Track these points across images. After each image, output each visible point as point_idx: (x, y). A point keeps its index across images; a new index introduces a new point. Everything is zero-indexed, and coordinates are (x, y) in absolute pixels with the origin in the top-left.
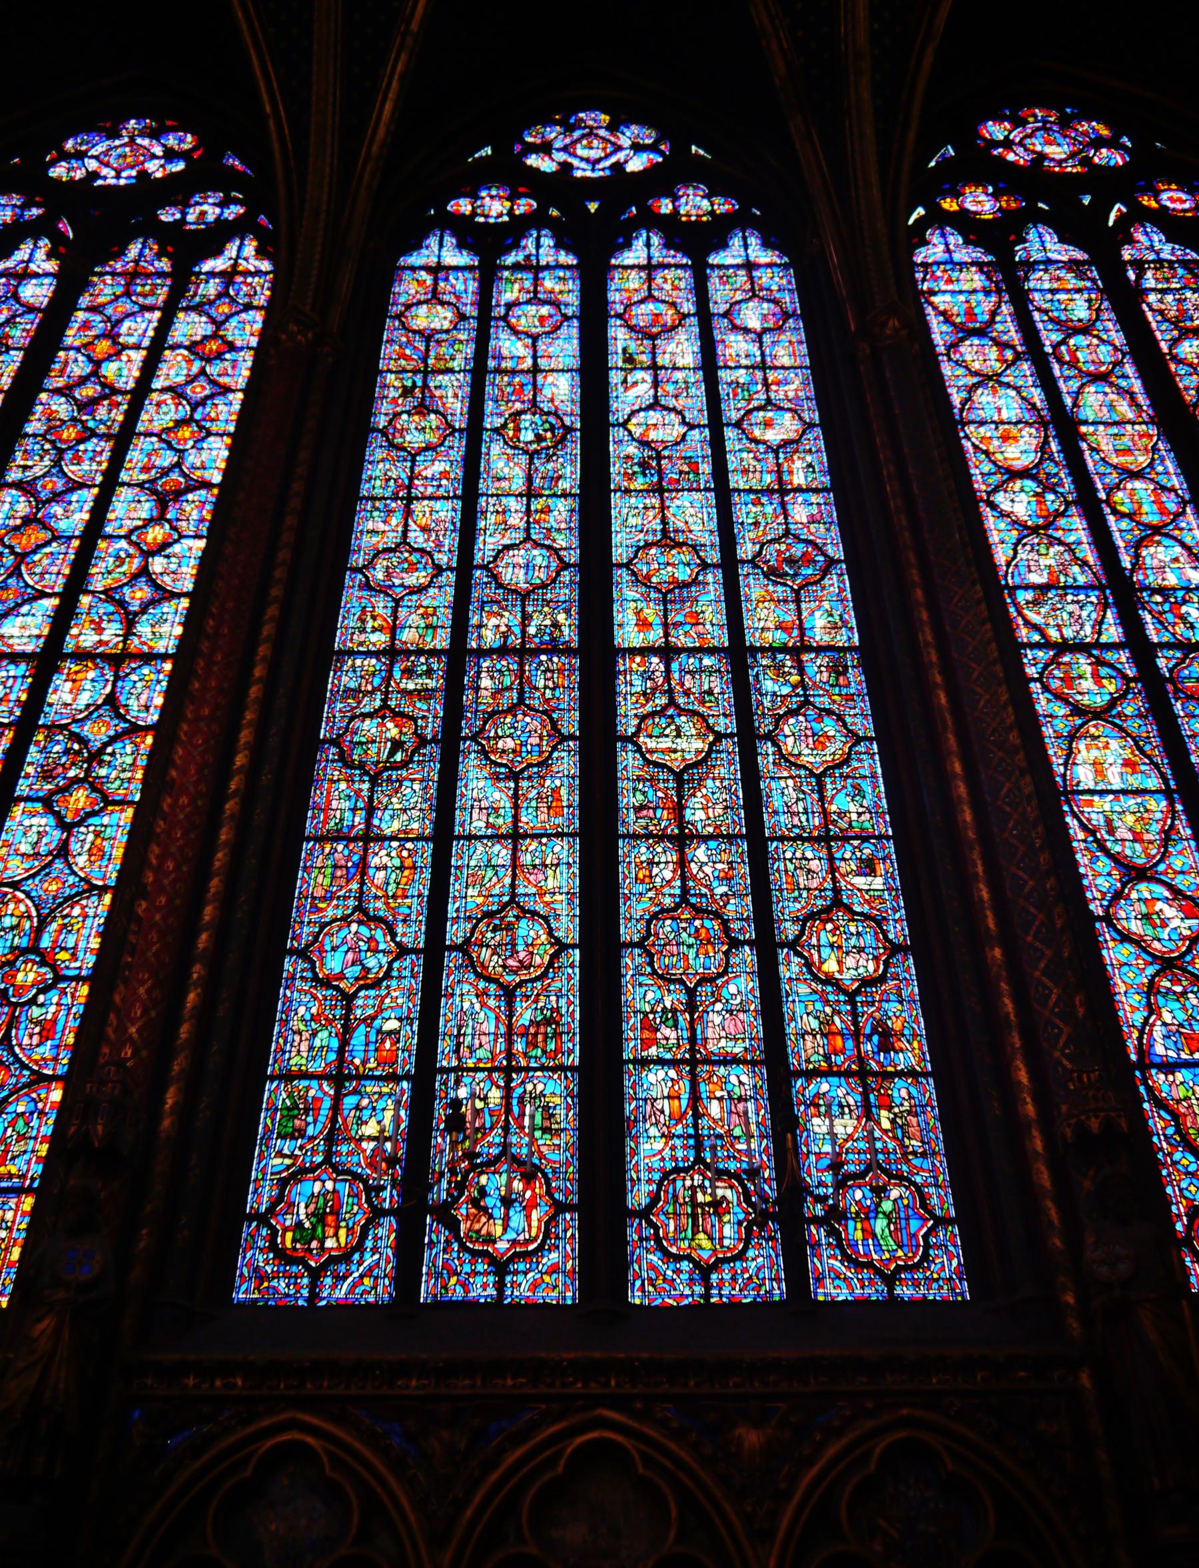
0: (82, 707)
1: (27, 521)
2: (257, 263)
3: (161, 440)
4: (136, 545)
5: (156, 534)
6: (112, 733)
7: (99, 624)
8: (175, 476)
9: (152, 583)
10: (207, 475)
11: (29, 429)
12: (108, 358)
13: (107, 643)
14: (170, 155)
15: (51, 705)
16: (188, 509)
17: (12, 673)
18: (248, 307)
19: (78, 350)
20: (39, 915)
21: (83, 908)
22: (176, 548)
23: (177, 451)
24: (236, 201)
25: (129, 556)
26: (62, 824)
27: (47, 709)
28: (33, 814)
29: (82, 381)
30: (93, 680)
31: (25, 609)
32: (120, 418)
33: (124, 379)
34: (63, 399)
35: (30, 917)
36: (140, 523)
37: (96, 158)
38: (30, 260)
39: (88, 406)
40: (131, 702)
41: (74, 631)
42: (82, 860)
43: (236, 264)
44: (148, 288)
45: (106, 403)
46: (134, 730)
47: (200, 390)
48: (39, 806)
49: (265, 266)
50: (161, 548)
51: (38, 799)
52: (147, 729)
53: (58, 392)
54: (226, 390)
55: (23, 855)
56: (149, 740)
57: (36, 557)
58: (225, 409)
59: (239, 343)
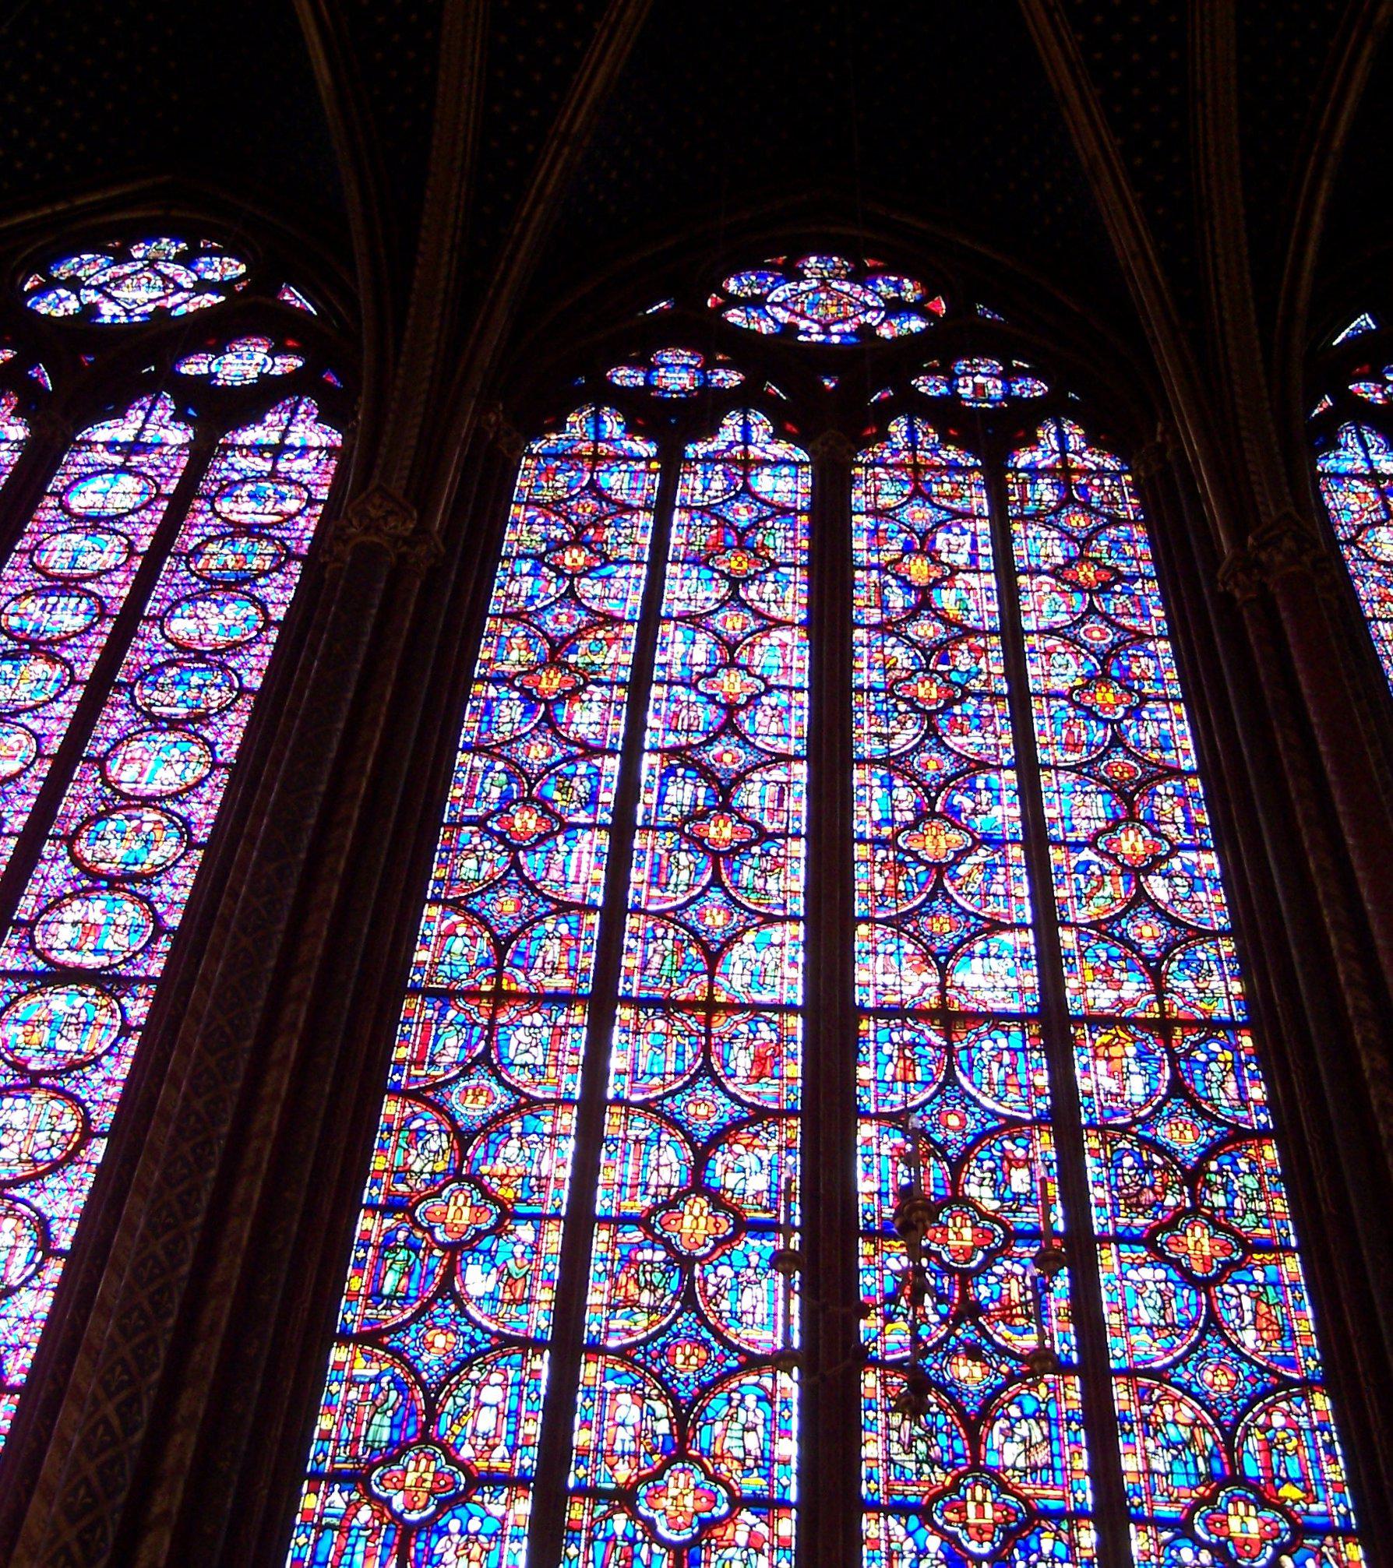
0: (1141, 1099)
1: (923, 815)
2: (1095, 458)
3: (1077, 706)
4: (1113, 858)
5: (1132, 843)
6: (1203, 1140)
7: (1109, 971)
8: (1118, 757)
9: (1158, 911)
10: (1169, 756)
11: (859, 680)
12: (936, 584)
13: (1133, 1003)
14: (895, 308)
15: (1089, 1095)
16: (1166, 806)
17: (1002, 1043)
18: (1115, 521)
19: (882, 569)
20: (1219, 1424)
21: (1287, 1415)
22: (1176, 864)
23: (1106, 722)
24: (1022, 373)
25: (1104, 872)
26: (1188, 1278)
27: (1086, 1101)
28: (1136, 1266)
29: (912, 614)
30: (1139, 1057)
31: (979, 947)
32: (999, 670)
33: (974, 615)
34: (893, 640)
35: (1205, 1426)
36: (1101, 825)
37: (783, 305)
38: (747, 440)
39: (941, 650)
40: (1214, 1093)
41: (1072, 983)
42: (1249, 1337)
43: (1064, 460)
44: (947, 487)
45: (963, 647)
46: (1235, 1137)
47: (1097, 635)
48: (1142, 1252)
49: (1110, 464)
50: (1155, 863)
51: (1133, 1240)
52: (1261, 1135)
53: (881, 628)
54: (1141, 637)
55: (1149, 1327)
56: (1271, 1153)
57: (962, 870)
58: (1152, 664)
59: (1124, 569)
